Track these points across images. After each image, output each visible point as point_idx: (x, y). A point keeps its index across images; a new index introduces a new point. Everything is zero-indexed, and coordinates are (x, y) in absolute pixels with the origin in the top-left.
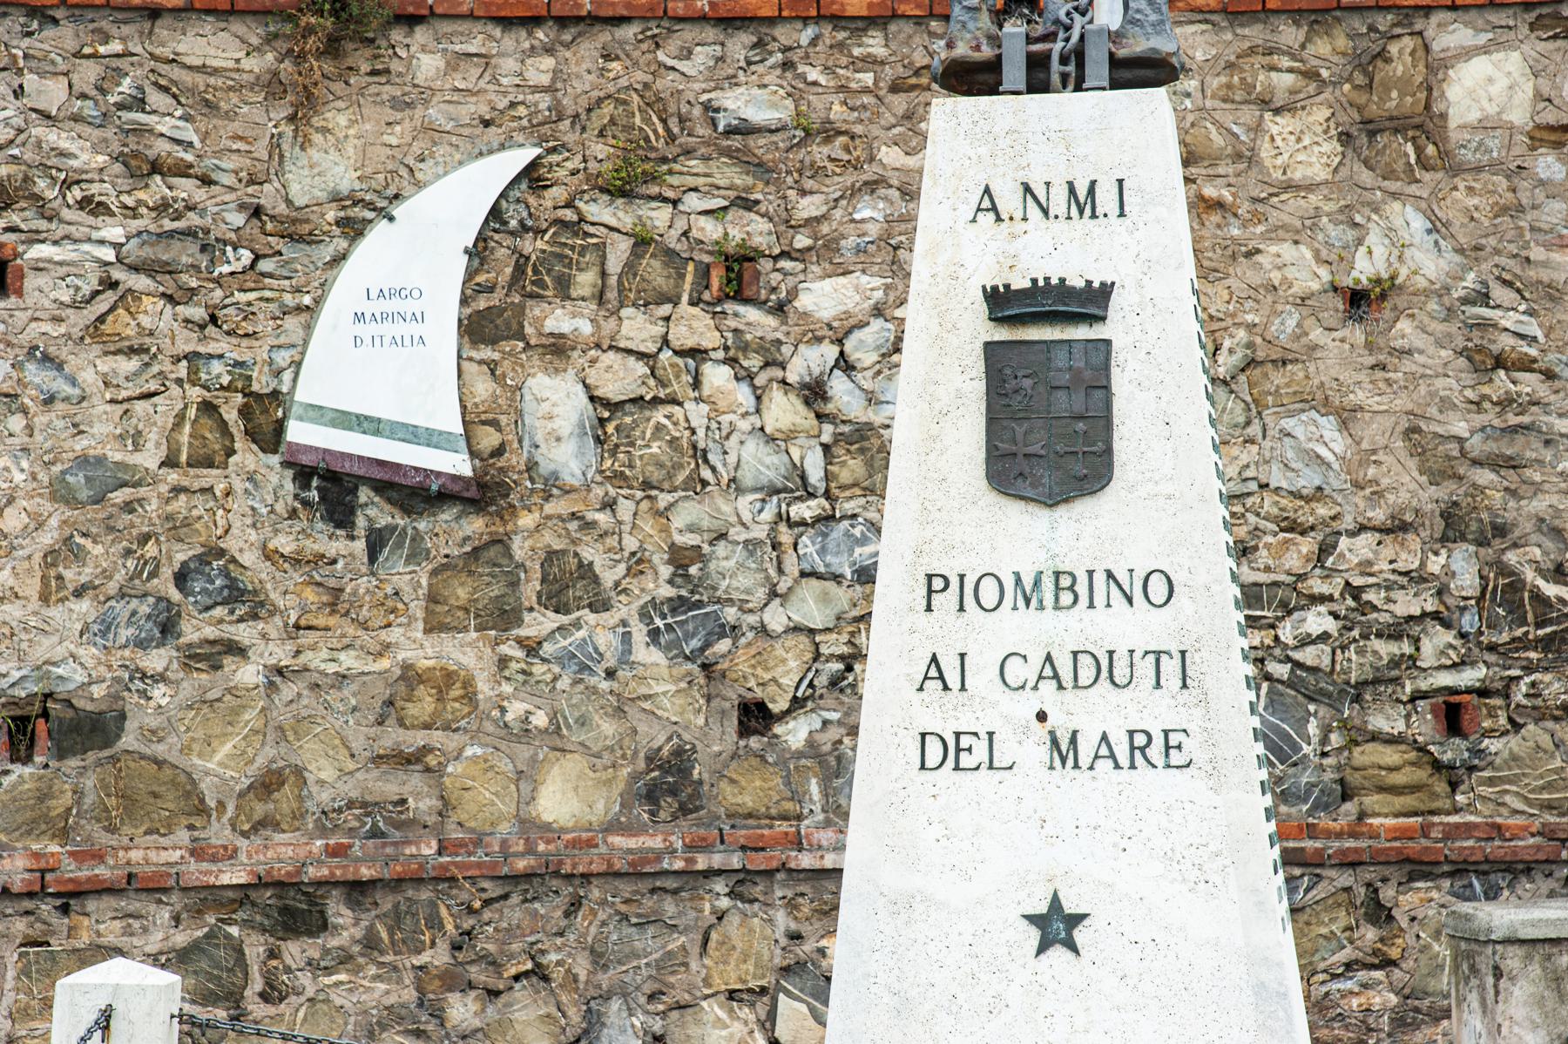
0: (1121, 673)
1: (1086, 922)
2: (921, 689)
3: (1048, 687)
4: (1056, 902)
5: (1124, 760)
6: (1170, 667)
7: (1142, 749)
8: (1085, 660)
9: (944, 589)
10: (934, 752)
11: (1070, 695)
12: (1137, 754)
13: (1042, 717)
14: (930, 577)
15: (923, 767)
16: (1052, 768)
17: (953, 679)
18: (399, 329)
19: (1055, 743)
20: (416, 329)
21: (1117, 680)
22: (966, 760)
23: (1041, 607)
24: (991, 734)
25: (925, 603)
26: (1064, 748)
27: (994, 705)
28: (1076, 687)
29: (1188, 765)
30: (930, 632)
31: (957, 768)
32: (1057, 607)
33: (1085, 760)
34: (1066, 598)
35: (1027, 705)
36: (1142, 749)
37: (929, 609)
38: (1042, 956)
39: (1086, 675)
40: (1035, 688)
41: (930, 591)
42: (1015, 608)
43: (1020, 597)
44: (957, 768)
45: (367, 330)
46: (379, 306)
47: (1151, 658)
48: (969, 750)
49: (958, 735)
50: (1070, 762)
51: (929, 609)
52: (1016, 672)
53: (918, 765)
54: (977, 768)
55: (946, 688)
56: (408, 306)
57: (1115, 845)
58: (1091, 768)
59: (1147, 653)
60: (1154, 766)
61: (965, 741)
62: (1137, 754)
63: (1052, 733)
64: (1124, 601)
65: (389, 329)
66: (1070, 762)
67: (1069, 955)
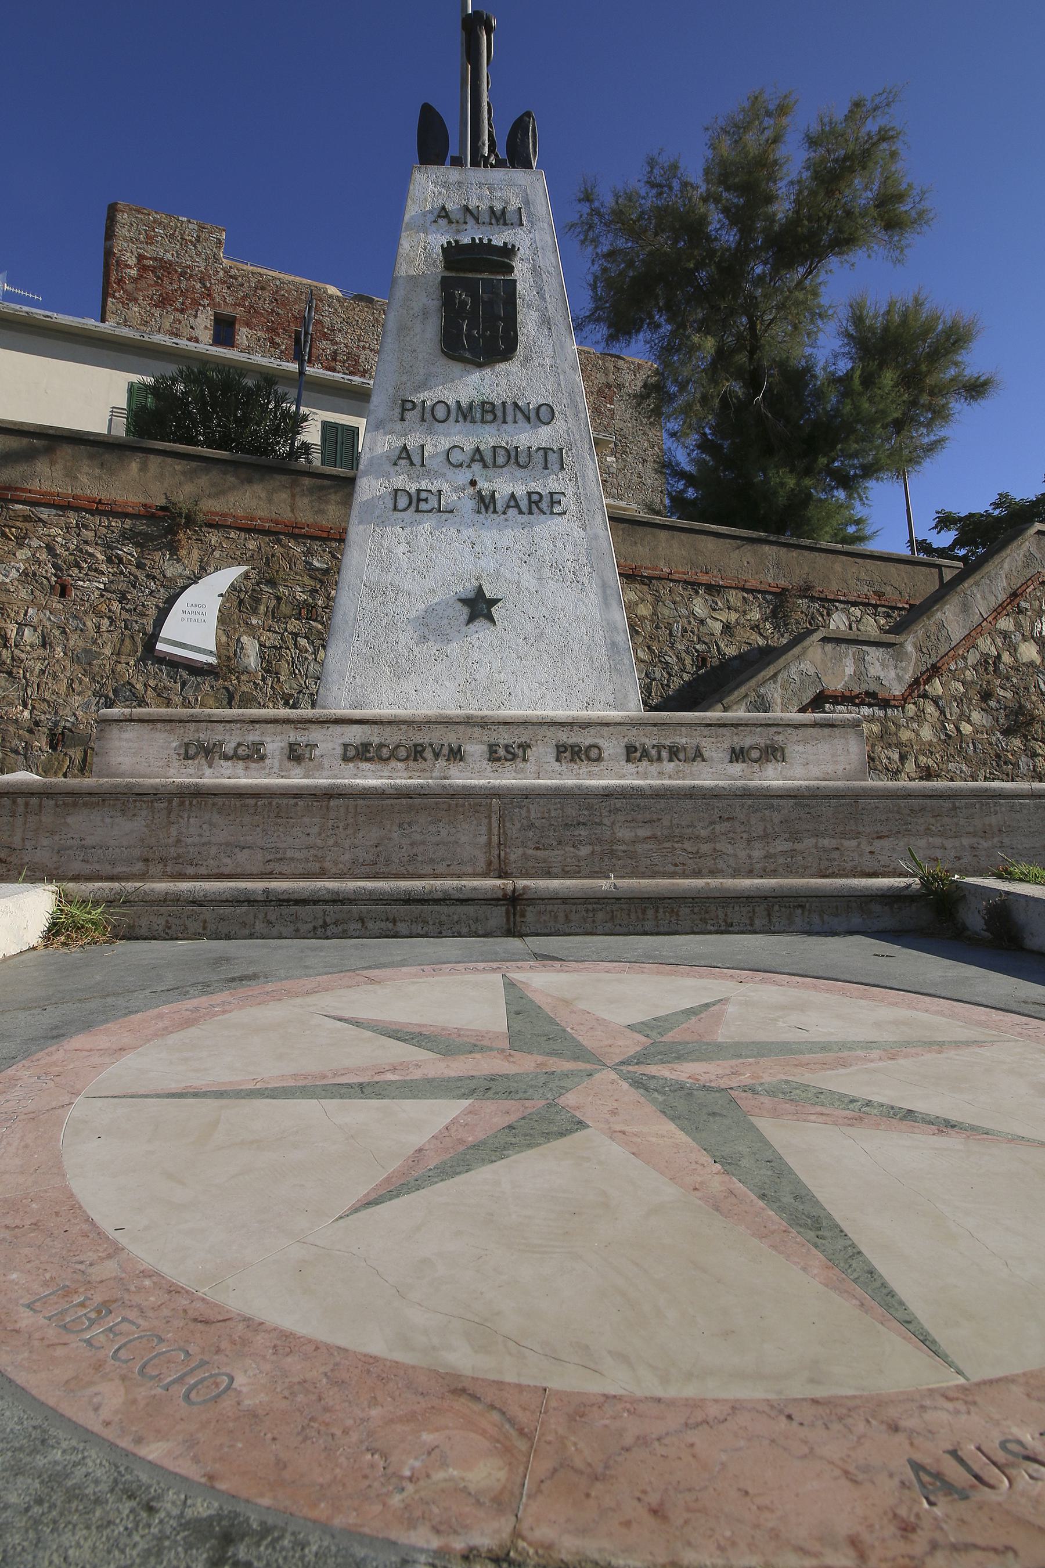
0: (522, 460)
1: (500, 604)
5: (524, 509)
6: (553, 457)
7: (537, 503)
9: (412, 409)
10: (403, 502)
11: (490, 472)
12: (534, 506)
13: (473, 483)
15: (395, 509)
16: (479, 512)
17: (416, 459)
18: (197, 617)
20: (203, 617)
22: (423, 506)
23: (473, 422)
24: (440, 491)
26: (487, 501)
28: (495, 465)
29: (565, 513)
32: (483, 421)
35: (463, 477)
36: (537, 503)
39: (501, 460)
40: (469, 466)
41: (404, 410)
44: (417, 511)
45: (186, 616)
46: (191, 609)
47: (541, 452)
49: (419, 491)
50: (491, 509)
51: (402, 419)
53: (392, 506)
54: (430, 511)
55: (412, 464)
56: (201, 610)
58: (504, 513)
59: (539, 449)
60: (545, 513)
62: (534, 506)
63: (479, 492)
65: (193, 616)
66: (491, 509)
67: (489, 624)
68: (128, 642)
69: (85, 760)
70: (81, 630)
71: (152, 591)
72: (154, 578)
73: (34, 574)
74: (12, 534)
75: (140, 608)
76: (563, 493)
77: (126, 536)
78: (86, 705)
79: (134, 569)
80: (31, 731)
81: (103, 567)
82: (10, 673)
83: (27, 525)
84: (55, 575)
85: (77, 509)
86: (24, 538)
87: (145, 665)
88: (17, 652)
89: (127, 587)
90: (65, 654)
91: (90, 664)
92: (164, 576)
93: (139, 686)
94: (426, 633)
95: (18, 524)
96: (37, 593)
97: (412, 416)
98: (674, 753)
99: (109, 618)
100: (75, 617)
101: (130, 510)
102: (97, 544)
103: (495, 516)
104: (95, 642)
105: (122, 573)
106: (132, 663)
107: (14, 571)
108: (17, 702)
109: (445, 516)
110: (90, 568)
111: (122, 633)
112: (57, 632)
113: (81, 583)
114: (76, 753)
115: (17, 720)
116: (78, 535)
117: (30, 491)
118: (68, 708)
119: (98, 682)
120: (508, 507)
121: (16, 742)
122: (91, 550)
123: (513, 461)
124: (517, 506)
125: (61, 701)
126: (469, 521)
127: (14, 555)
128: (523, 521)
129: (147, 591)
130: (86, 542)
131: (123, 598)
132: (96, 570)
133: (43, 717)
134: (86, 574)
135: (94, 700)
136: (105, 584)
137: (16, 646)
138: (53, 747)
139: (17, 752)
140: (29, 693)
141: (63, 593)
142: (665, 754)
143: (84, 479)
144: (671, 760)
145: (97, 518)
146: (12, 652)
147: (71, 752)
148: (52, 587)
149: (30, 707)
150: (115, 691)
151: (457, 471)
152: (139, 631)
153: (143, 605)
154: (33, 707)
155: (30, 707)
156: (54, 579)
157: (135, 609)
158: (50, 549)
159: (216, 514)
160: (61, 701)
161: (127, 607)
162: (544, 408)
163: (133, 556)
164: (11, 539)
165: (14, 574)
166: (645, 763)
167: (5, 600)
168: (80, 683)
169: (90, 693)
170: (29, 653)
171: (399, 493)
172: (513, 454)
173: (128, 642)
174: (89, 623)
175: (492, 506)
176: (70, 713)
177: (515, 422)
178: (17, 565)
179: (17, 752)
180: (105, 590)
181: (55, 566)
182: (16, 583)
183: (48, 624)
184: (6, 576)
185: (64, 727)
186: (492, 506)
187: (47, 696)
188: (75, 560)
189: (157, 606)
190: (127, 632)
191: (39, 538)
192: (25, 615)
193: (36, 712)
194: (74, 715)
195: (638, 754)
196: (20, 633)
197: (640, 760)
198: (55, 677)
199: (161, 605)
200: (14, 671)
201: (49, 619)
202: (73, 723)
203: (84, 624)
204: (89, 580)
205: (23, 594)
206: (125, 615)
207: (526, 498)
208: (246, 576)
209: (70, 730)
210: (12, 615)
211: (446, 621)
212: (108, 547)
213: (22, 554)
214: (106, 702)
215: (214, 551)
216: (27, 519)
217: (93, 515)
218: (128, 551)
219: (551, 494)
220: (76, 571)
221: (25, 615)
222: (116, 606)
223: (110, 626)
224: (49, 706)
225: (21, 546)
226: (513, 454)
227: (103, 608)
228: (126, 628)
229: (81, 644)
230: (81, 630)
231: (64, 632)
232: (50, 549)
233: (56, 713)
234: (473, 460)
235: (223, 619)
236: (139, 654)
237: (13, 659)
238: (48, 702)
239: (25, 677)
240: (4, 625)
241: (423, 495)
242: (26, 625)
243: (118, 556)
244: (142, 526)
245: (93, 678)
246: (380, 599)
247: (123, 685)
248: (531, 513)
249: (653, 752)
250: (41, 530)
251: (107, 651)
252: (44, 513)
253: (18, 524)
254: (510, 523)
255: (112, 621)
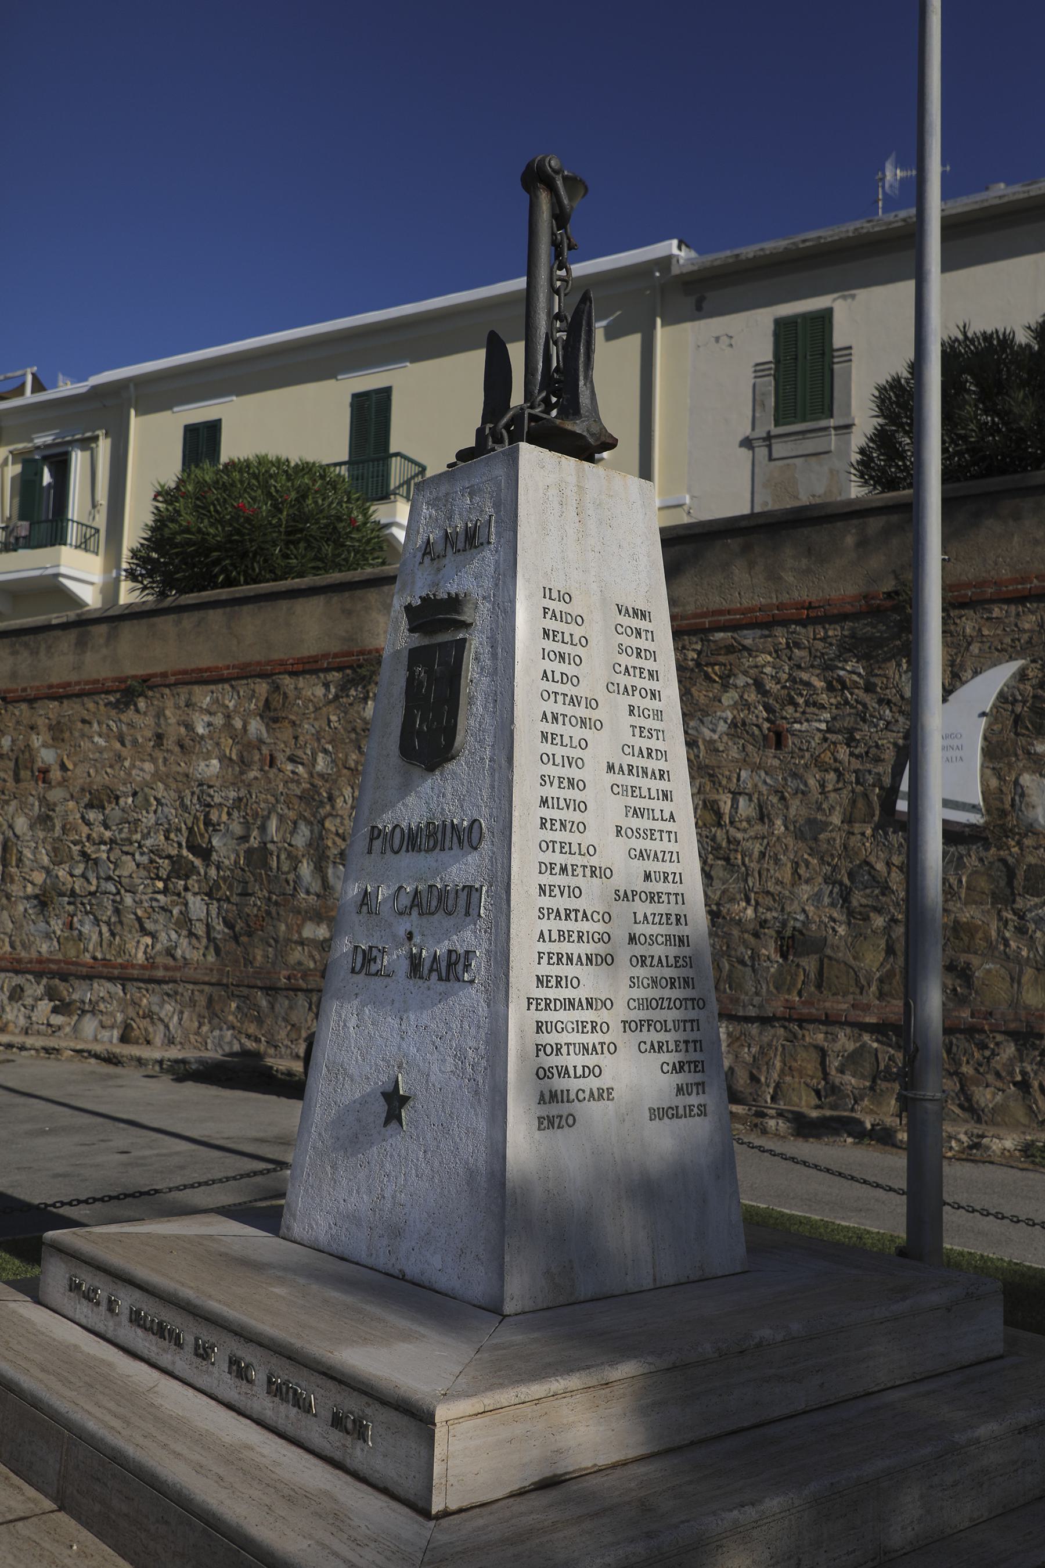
20: (958, 753)
68: (861, 804)
69: (820, 972)
70: (803, 793)
71: (888, 723)
72: (889, 702)
73: (744, 724)
74: (716, 674)
75: (873, 750)
77: (849, 647)
78: (817, 897)
79: (860, 693)
80: (756, 935)
81: (824, 698)
82: (727, 859)
83: (731, 657)
84: (768, 720)
85: (784, 623)
86: (729, 676)
87: (886, 834)
88: (732, 831)
89: (856, 722)
90: (787, 828)
91: (816, 839)
92: (902, 697)
93: (880, 866)
95: (722, 659)
96: (750, 748)
99: (836, 770)
100: (795, 775)
101: (848, 609)
102: (812, 666)
104: (819, 808)
105: (847, 702)
106: (869, 832)
107: (722, 723)
108: (738, 897)
110: (807, 703)
111: (853, 791)
112: (774, 799)
113: (797, 726)
114: (810, 963)
115: (740, 920)
116: (790, 659)
117: (729, 612)
118: (796, 902)
119: (829, 864)
121: (742, 949)
122: (805, 676)
125: (787, 893)
127: (720, 701)
129: (882, 724)
130: (799, 667)
131: (850, 741)
132: (815, 704)
133: (769, 915)
134: (804, 713)
135: (827, 889)
136: (827, 722)
137: (732, 823)
138: (784, 956)
139: (742, 962)
140: (751, 884)
141: (779, 744)
143: (789, 578)
145: (810, 629)
146: (727, 832)
147: (804, 962)
148: (765, 737)
149: (753, 902)
150: (851, 875)
152: (874, 785)
153: (877, 746)
154: (757, 903)
155: (753, 902)
156: (766, 725)
157: (867, 753)
158: (759, 685)
159: (968, 585)
160: (787, 893)
161: (857, 751)
163: (859, 675)
164: (715, 681)
165: (722, 727)
167: (714, 763)
168: (807, 867)
169: (820, 879)
170: (745, 830)
173: (861, 804)
174: (812, 782)
176: (799, 910)
178: (724, 715)
179: (742, 962)
180: (829, 730)
181: (768, 708)
182: (725, 738)
183: (764, 789)
184: (714, 731)
185: (794, 928)
187: (771, 887)
188: (789, 695)
189: (895, 744)
190: (859, 789)
191: (745, 673)
192: (738, 780)
193: (761, 910)
194: (804, 911)
196: (735, 806)
198: (777, 861)
199: (901, 742)
200: (732, 857)
201: (765, 782)
202: (803, 922)
203: (806, 784)
204: (807, 720)
205: (734, 753)
206: (856, 764)
208: (1022, 675)
209: (801, 932)
210: (724, 782)
212: (828, 667)
213: (729, 698)
214: (841, 890)
215: (969, 644)
216: (730, 649)
217: (805, 626)
218: (852, 669)
220: (790, 709)
221: (738, 780)
222: (843, 752)
223: (838, 781)
224: (774, 900)
225: (725, 687)
227: (827, 757)
228: (858, 782)
229: (804, 812)
230: (803, 793)
231: (783, 798)
232: (759, 685)
233: (783, 910)
235: (993, 751)
236: (876, 818)
237: (729, 842)
238: (772, 895)
239: (744, 864)
240: (717, 797)
242: (740, 794)
243: (841, 680)
244: (864, 628)
245: (822, 859)
247: (860, 866)
250: (747, 662)
251: (836, 819)
252: (748, 637)
253: (722, 659)
255: (840, 775)
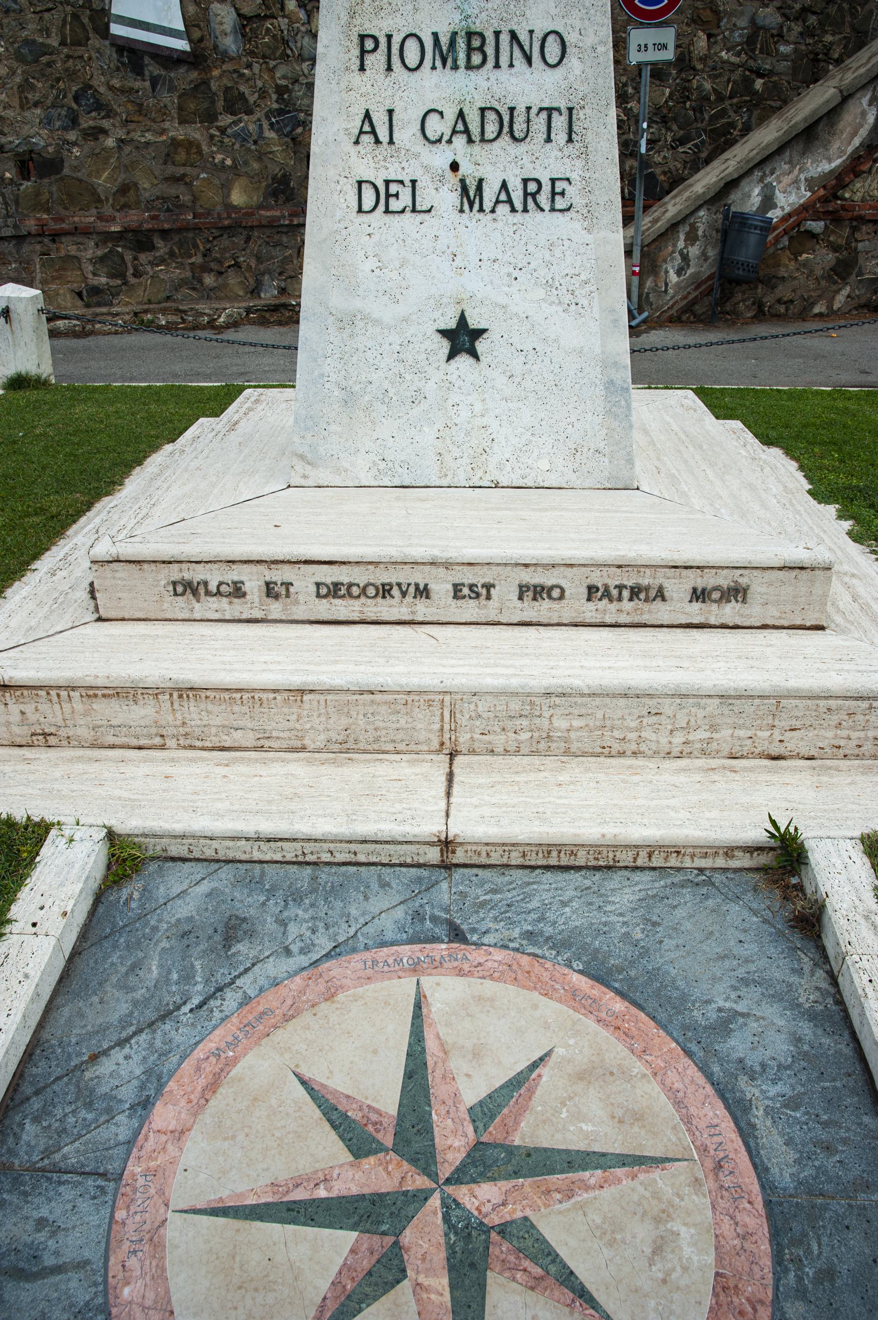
0: (519, 127)
2: (357, 142)
3: (460, 141)
4: (462, 319)
5: (519, 205)
6: (559, 122)
8: (491, 116)
9: (375, 50)
11: (477, 148)
12: (530, 200)
13: (454, 167)
14: (362, 38)
15: (360, 210)
16: (462, 211)
17: (383, 133)
19: (465, 190)
21: (517, 134)
22: (394, 205)
23: (455, 67)
24: (414, 182)
25: (358, 62)
26: (472, 194)
27: (417, 156)
28: (483, 140)
29: (568, 209)
30: (363, 90)
31: (387, 211)
32: (469, 67)
33: (488, 205)
34: (476, 59)
35: (441, 157)
36: (534, 195)
37: (362, 68)
38: (452, 362)
39: (491, 129)
40: (450, 141)
41: (363, 52)
42: (434, 68)
43: (437, 57)
44: (387, 211)
47: (544, 115)
48: (397, 196)
49: (387, 183)
50: (476, 206)
51: (362, 68)
52: (435, 126)
54: (403, 211)
55: (377, 141)
57: (509, 275)
58: (493, 211)
59: (541, 109)
60: (542, 210)
61: (393, 188)
62: (530, 200)
63: (462, 181)
64: (524, 61)
66: (476, 206)
76: (568, 180)
94: (402, 371)
97: (375, 61)
98: (635, 592)
103: (481, 216)
109: (420, 217)
120: (498, 202)
123: (506, 129)
124: (510, 201)
126: (449, 223)
128: (515, 221)
142: (626, 594)
144: (631, 599)
151: (434, 148)
162: (551, 39)
166: (605, 601)
171: (364, 186)
172: (506, 119)
175: (477, 201)
177: (511, 65)
186: (477, 201)
195: (599, 594)
197: (600, 600)
207: (520, 186)
211: (424, 356)
219: (553, 181)
226: (506, 119)
234: (454, 132)
241: (393, 188)
246: (348, 331)
248: (525, 210)
249: (615, 592)
254: (500, 225)
